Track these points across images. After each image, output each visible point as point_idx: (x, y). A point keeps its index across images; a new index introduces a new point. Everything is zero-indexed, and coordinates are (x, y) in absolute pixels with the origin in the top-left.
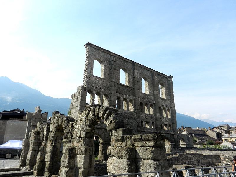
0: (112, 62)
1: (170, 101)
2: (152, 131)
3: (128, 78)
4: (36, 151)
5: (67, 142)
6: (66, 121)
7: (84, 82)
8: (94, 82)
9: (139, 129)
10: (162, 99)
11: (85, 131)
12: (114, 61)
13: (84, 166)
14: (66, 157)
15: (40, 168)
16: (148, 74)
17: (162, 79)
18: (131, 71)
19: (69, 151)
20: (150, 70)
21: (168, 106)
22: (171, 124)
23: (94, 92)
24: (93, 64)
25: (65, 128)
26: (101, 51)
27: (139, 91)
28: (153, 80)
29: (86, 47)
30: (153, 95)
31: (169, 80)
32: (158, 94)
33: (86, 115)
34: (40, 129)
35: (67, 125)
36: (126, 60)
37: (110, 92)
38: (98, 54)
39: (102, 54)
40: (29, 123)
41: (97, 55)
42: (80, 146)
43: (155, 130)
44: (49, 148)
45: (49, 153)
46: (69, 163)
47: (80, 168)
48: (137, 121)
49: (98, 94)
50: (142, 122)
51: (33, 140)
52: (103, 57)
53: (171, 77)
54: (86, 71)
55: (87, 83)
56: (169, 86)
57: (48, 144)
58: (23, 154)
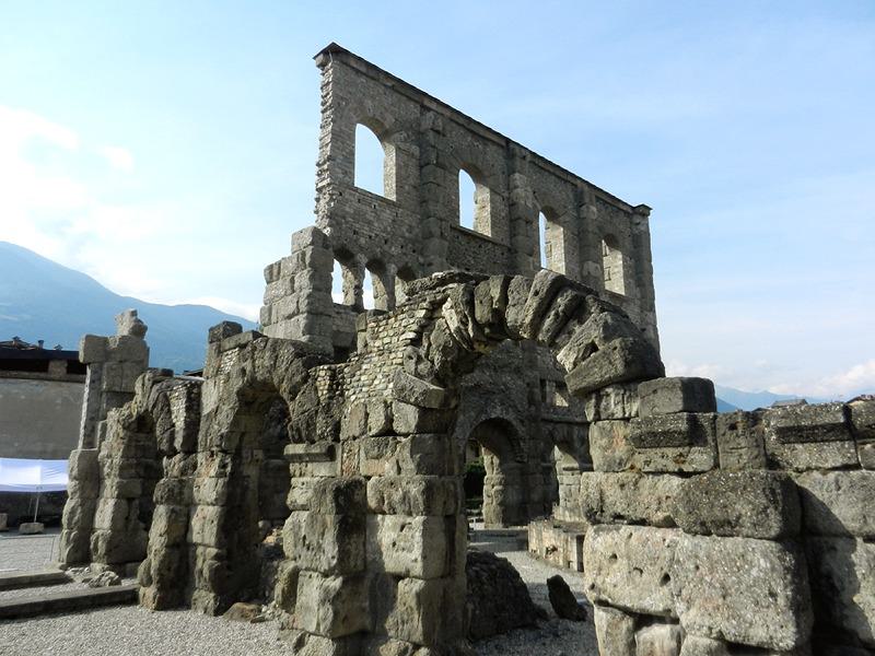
0: (431, 135)
1: (641, 307)
3: (489, 208)
4: (133, 499)
5: (308, 455)
6: (298, 363)
7: (316, 212)
8: (358, 216)
9: (533, 408)
11: (416, 404)
12: (438, 132)
13: (425, 568)
14: (324, 525)
15: (172, 574)
16: (561, 195)
18: (501, 178)
19: (336, 498)
20: (569, 178)
23: (363, 259)
24: (352, 137)
25: (294, 393)
26: (385, 85)
27: (531, 259)
28: (578, 218)
29: (322, 66)
32: (598, 274)
33: (415, 327)
34: (154, 406)
35: (305, 380)
36: (482, 132)
37: (421, 260)
39: (390, 99)
40: (92, 381)
41: (369, 103)
42: (391, 474)
44: (208, 485)
45: (211, 508)
46: (343, 555)
47: (399, 577)
48: (527, 380)
49: (377, 267)
50: (543, 382)
51: (120, 454)
53: (643, 211)
54: (325, 167)
55: (333, 217)
56: (635, 247)
57: (201, 469)
58: (73, 512)
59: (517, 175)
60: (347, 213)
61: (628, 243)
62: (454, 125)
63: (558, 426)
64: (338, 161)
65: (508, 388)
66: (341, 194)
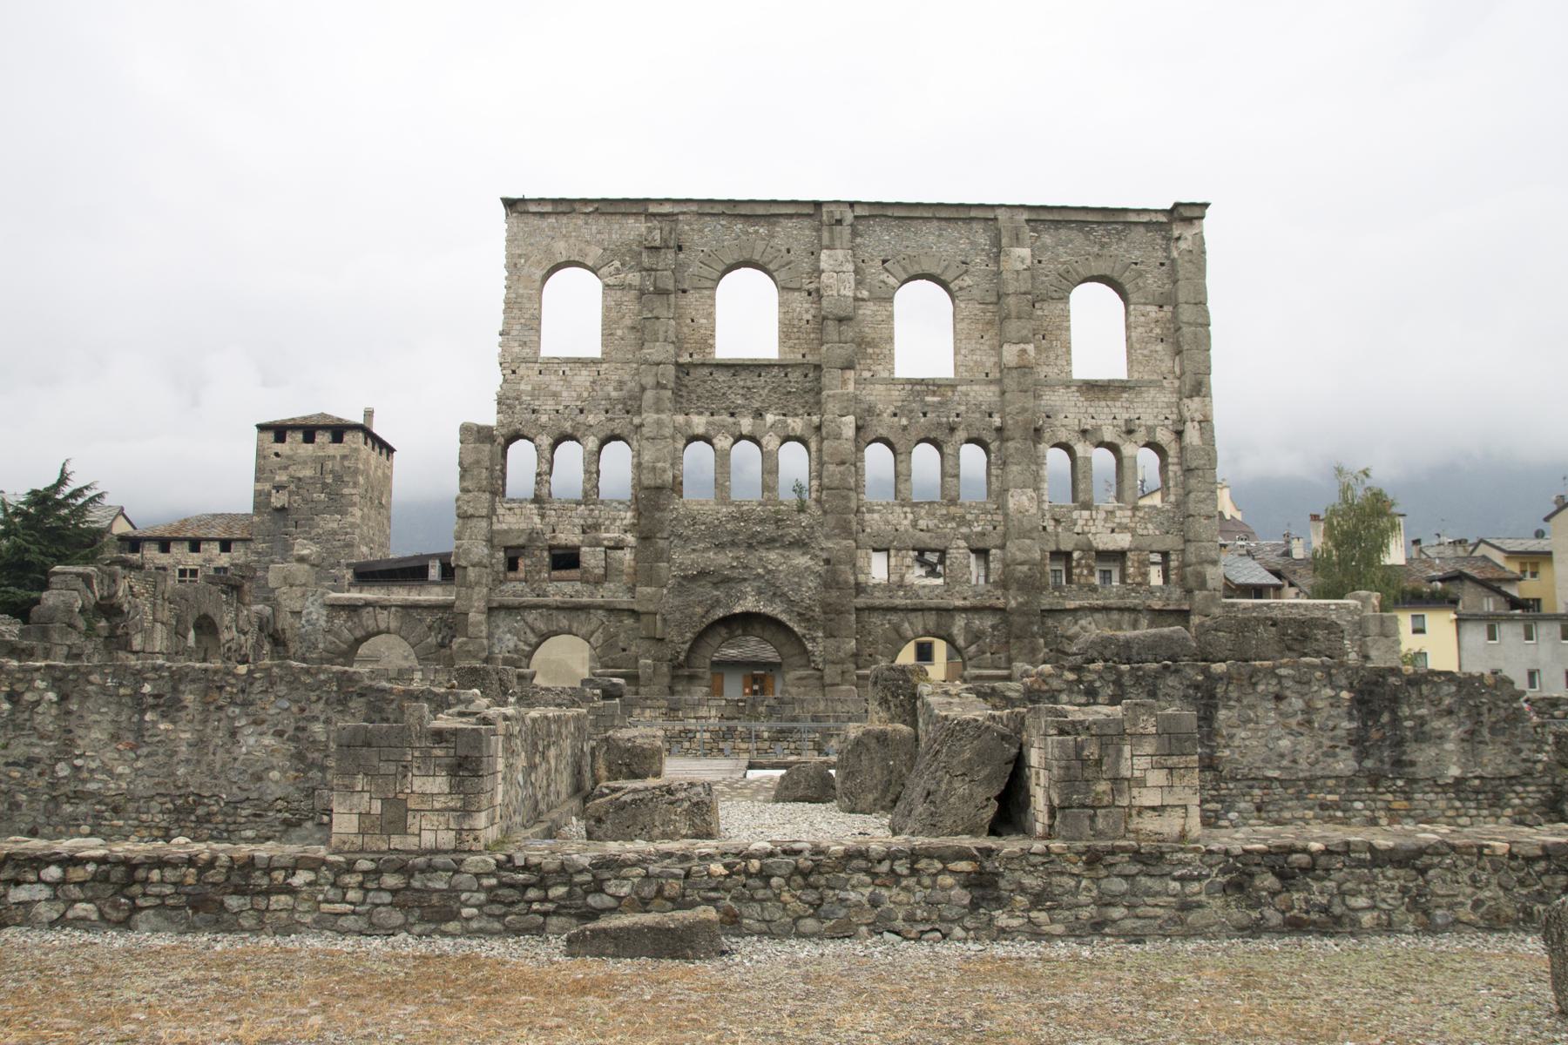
2: (959, 603)
10: (1093, 388)
17: (1103, 246)
20: (973, 214)
21: (1151, 430)
22: (1171, 542)
27: (850, 374)
30: (995, 374)
31: (1178, 239)
36: (760, 210)
39: (596, 225)
43: (999, 593)
48: (825, 555)
52: (600, 243)
59: (824, 255)
60: (522, 392)
61: (1154, 281)
63: (912, 616)
64: (514, 333)
65: (769, 572)
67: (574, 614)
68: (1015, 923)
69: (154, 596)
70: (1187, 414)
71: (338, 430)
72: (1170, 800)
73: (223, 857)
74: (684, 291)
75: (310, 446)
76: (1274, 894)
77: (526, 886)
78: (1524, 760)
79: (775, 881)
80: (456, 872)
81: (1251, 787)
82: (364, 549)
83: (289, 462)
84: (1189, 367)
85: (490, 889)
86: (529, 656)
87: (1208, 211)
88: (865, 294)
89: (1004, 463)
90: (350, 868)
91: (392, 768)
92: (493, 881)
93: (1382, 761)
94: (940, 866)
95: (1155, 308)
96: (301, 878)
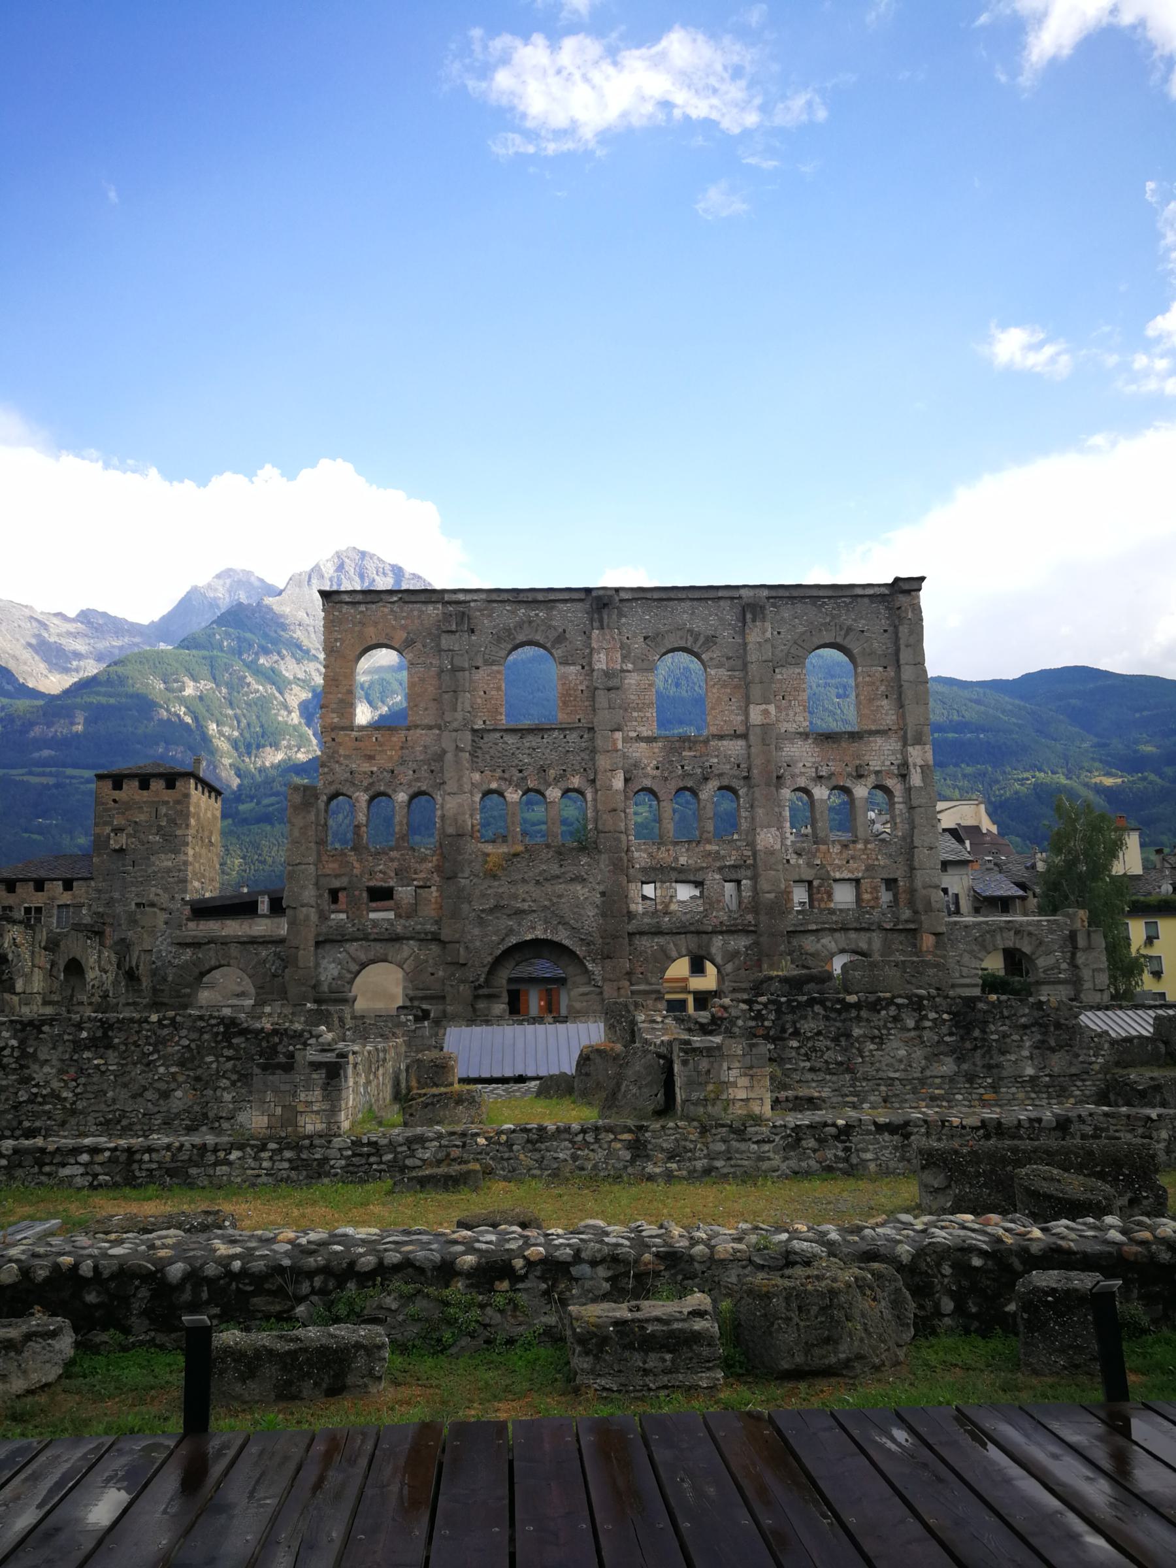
17: (833, 617)
20: (720, 594)
22: (899, 873)
38: (376, 624)
52: (404, 627)
62: (495, 605)
66: (333, 740)
67: (390, 944)
68: (658, 1170)
69: (33, 945)
70: (910, 760)
71: (171, 780)
72: (751, 1095)
73: (187, 1145)
74: (477, 668)
75: (145, 793)
76: (815, 1151)
77: (369, 1155)
78: (1082, 1062)
79: (515, 1147)
80: (328, 1148)
81: (879, 1085)
82: (196, 884)
83: (127, 806)
84: (911, 720)
85: (348, 1158)
86: (351, 982)
87: (924, 584)
88: (630, 667)
89: (752, 806)
90: (263, 1148)
91: (287, 1087)
92: (350, 1153)
93: (975, 1065)
94: (612, 1137)
95: (881, 669)
96: (234, 1155)
